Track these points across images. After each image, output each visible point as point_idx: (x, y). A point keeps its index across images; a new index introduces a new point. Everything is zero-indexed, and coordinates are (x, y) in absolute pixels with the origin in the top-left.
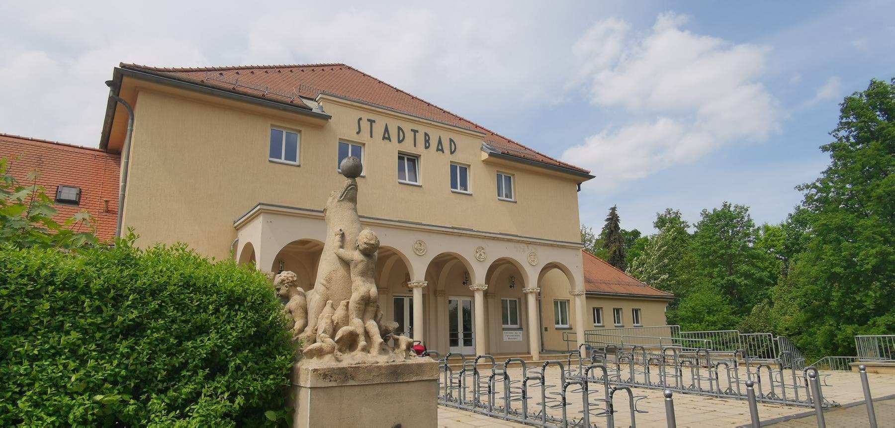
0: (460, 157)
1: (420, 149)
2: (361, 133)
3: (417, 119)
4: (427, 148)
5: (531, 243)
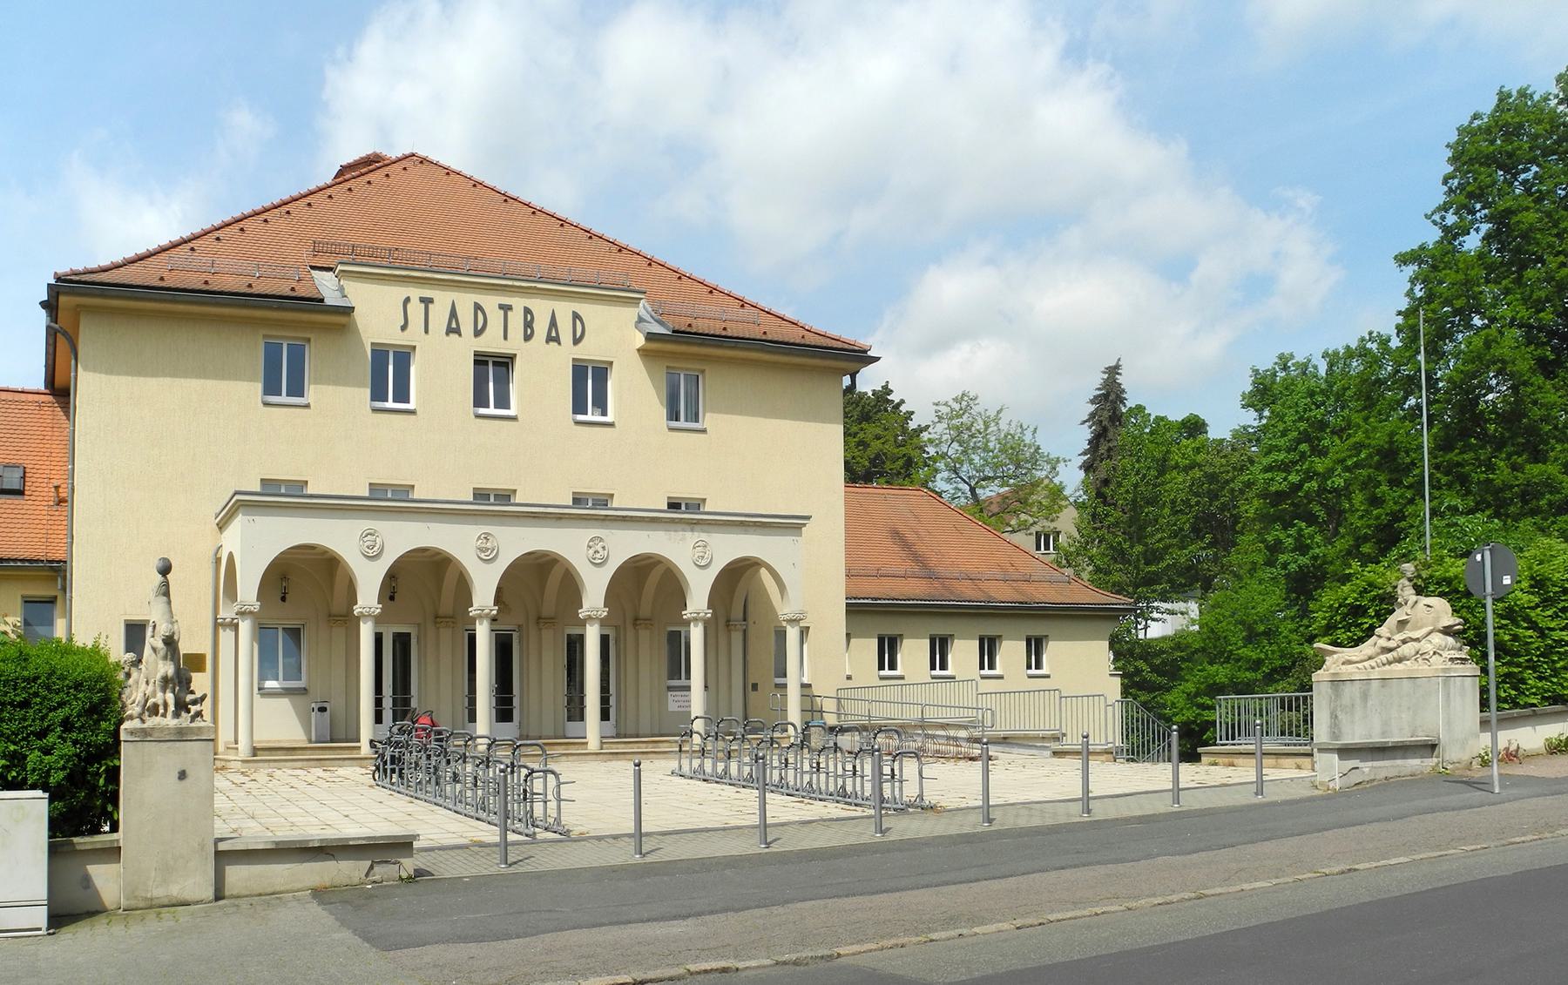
3: (510, 283)
4: (527, 338)
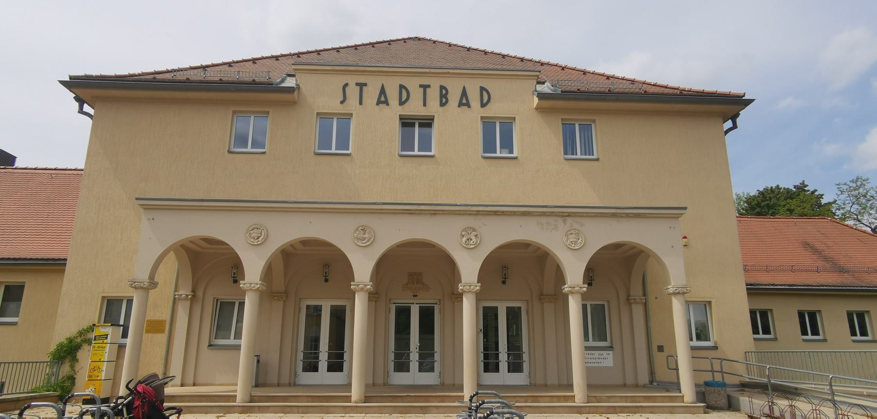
0: (496, 109)
1: (433, 108)
5: (569, 215)
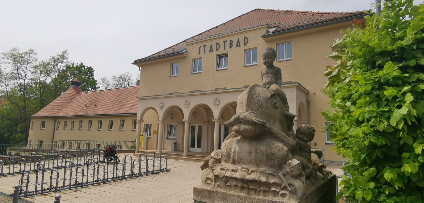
0: (250, 45)
2: (200, 53)
3: (225, 35)
4: (230, 47)
